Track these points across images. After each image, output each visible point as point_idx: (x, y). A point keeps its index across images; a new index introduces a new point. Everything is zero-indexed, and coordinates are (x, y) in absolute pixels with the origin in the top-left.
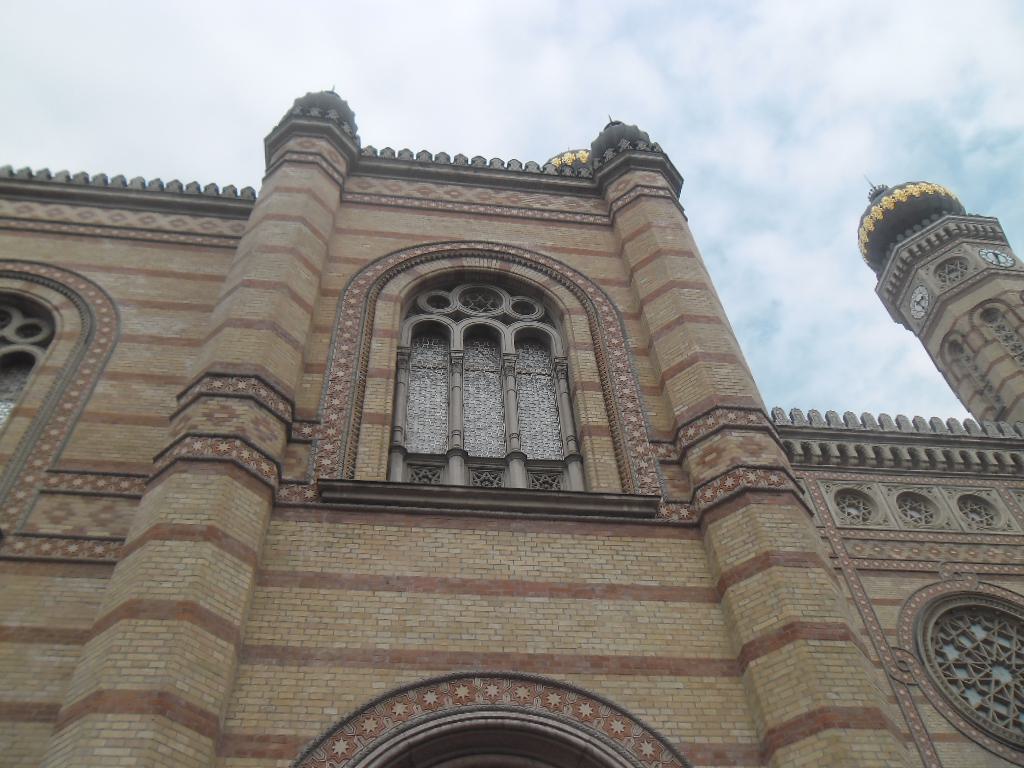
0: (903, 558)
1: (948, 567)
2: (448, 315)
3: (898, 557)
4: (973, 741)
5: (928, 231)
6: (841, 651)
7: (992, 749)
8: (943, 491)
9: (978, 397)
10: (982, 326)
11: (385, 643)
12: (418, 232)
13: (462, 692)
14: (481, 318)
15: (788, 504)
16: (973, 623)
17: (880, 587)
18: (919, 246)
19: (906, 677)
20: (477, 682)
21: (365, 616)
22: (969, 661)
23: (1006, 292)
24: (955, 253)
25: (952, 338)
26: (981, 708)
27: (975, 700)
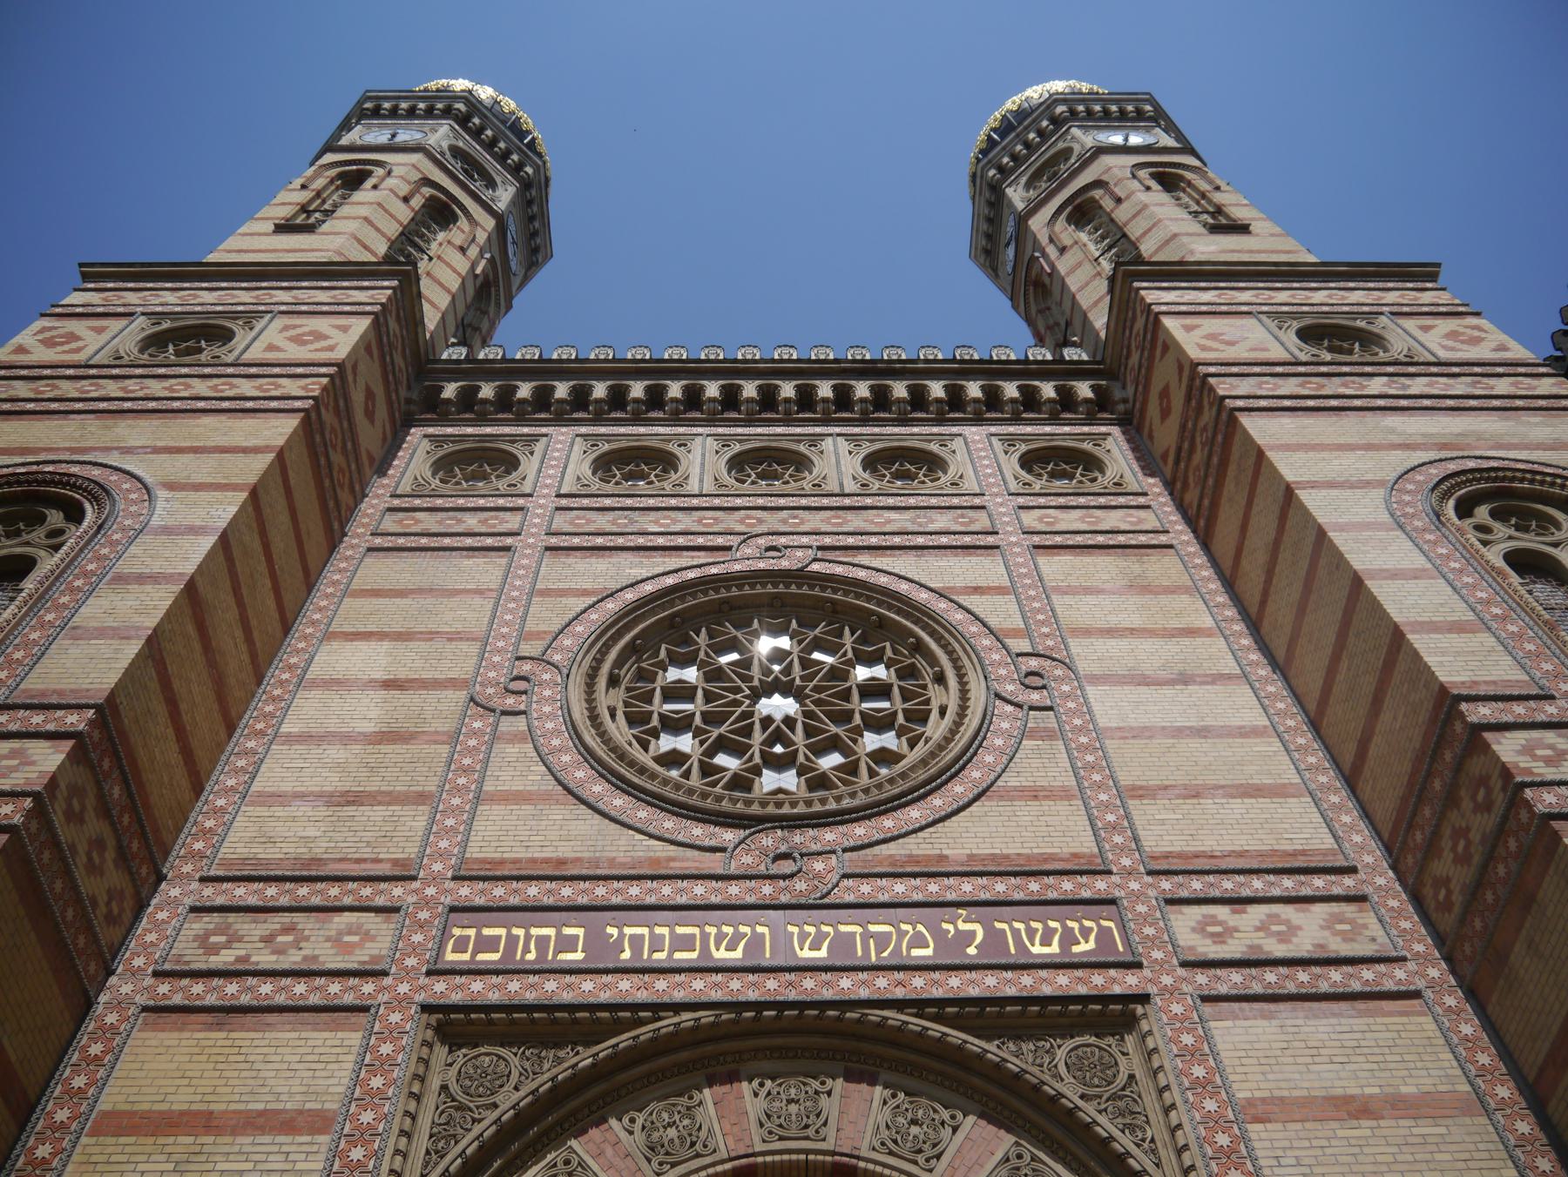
1: (762, 541)
5: (1026, 128)
16: (776, 632)
19: (510, 701)
26: (674, 759)
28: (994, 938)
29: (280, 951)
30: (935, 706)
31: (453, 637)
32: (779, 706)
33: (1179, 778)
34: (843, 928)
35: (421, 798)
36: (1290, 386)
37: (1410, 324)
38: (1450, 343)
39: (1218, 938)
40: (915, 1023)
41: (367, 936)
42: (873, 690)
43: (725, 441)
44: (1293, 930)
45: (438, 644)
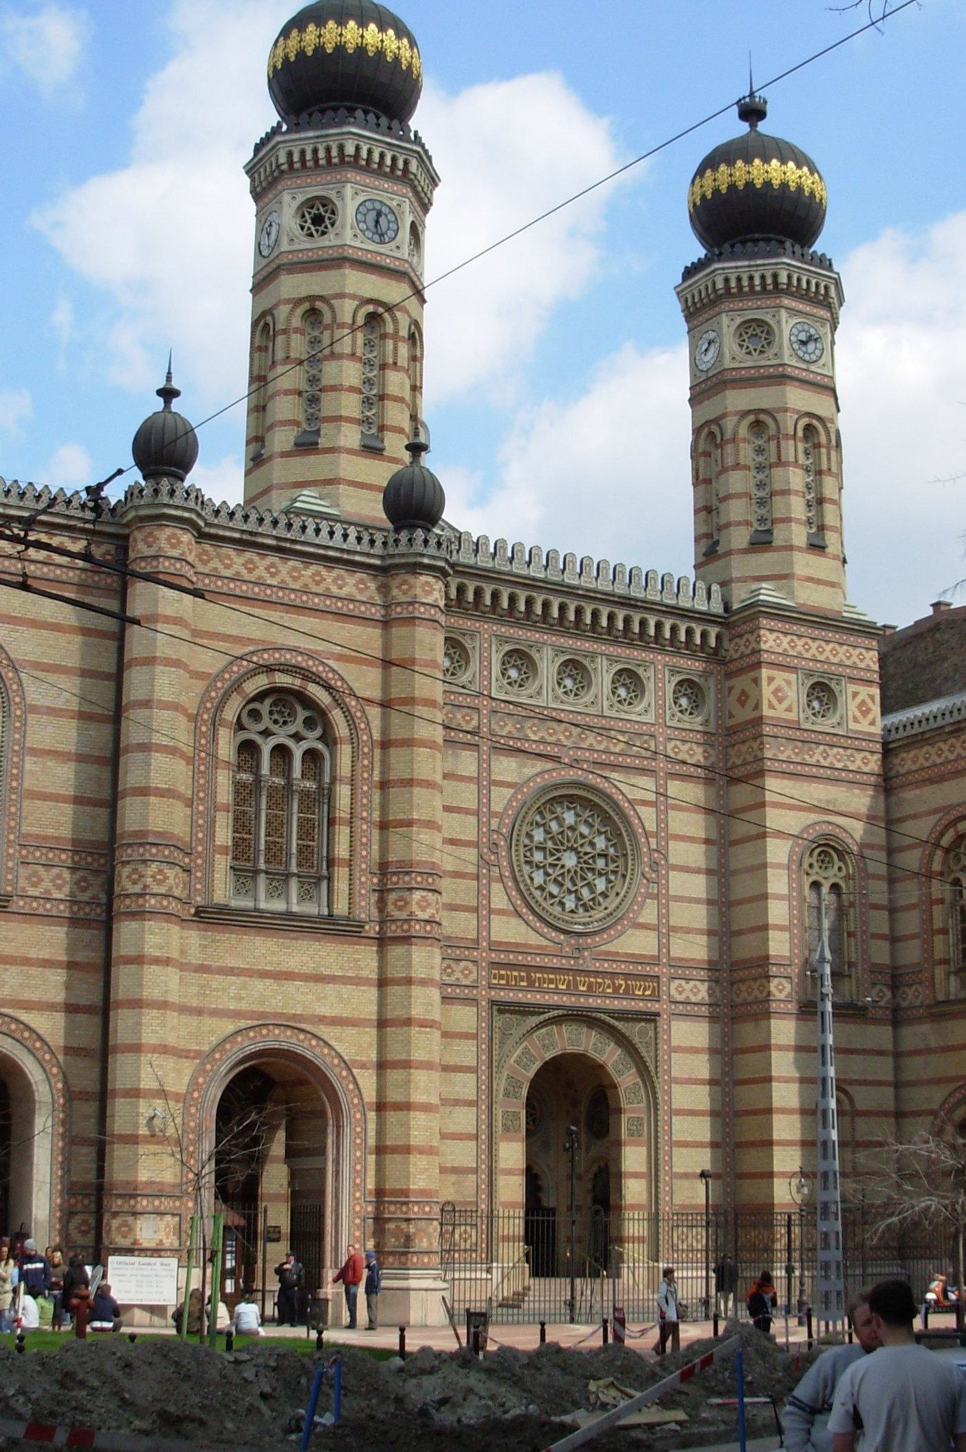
0: (537, 739)
1: (571, 753)
2: (261, 733)
3: (533, 737)
4: (520, 916)
5: (757, 266)
6: (427, 1033)
7: (532, 924)
8: (605, 662)
9: (704, 513)
10: (745, 440)
11: (232, 1006)
12: (245, 633)
13: (264, 1032)
14: (281, 738)
15: (430, 946)
17: (506, 768)
18: (739, 279)
19: (493, 858)
20: (271, 1027)
21: (224, 990)
22: (550, 844)
23: (786, 410)
24: (768, 318)
25: (714, 428)
26: (542, 888)
27: (539, 878)
28: (627, 985)
29: (449, 976)
30: (621, 870)
31: (467, 812)
32: (570, 860)
33: (685, 924)
34: (592, 980)
35: (476, 910)
36: (787, 753)
37: (852, 688)
38: (858, 714)
39: (680, 993)
40: (608, 1019)
41: (471, 972)
42: (604, 855)
43: (559, 651)
44: (699, 991)
45: (463, 816)
